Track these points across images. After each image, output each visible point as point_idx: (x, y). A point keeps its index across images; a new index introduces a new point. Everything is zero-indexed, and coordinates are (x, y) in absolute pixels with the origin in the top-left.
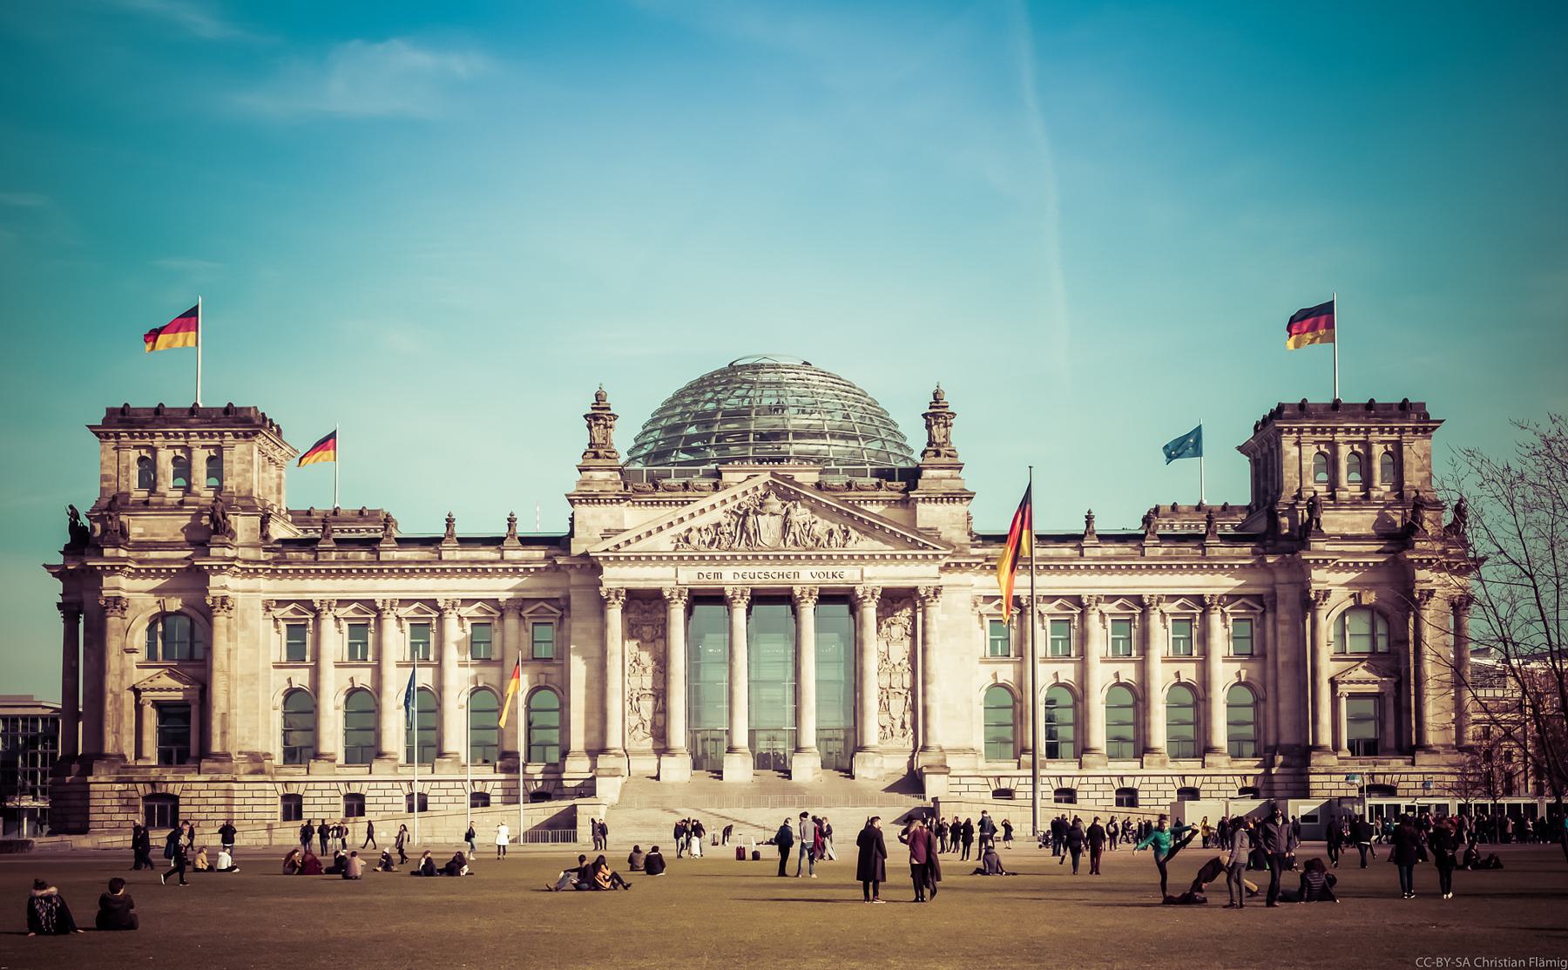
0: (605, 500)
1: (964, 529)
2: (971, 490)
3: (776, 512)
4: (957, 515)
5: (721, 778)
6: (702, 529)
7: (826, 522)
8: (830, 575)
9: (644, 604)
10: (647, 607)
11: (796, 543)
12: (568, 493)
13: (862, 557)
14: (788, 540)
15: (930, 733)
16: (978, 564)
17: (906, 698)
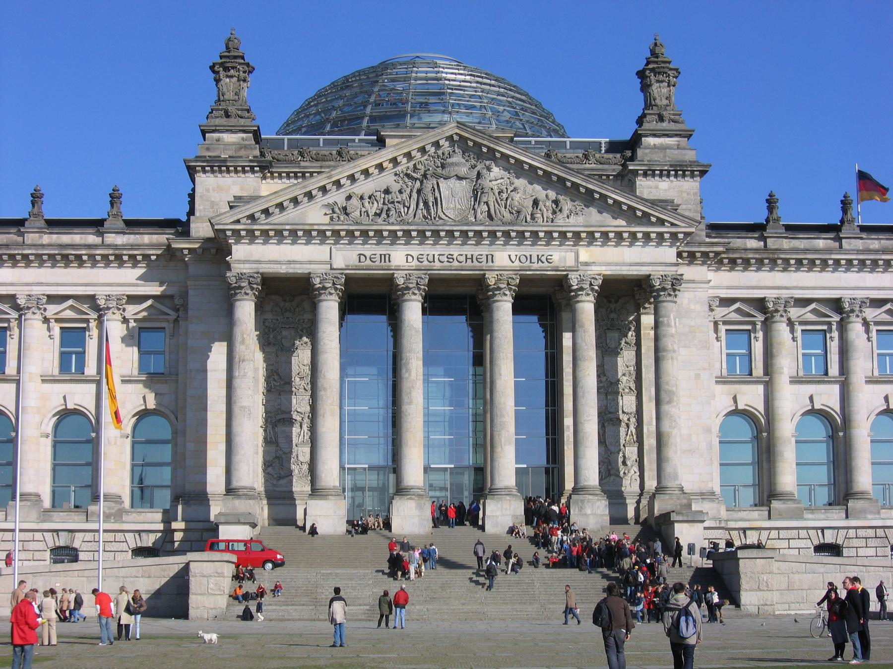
0: (235, 167)
1: (696, 211)
2: (704, 162)
3: (461, 174)
4: (688, 194)
5: (390, 530)
6: (366, 197)
7: (530, 188)
8: (535, 259)
9: (285, 301)
10: (288, 304)
11: (490, 217)
12: (187, 158)
13: (577, 235)
14: (479, 212)
15: (668, 469)
16: (717, 254)
17: (628, 426)
